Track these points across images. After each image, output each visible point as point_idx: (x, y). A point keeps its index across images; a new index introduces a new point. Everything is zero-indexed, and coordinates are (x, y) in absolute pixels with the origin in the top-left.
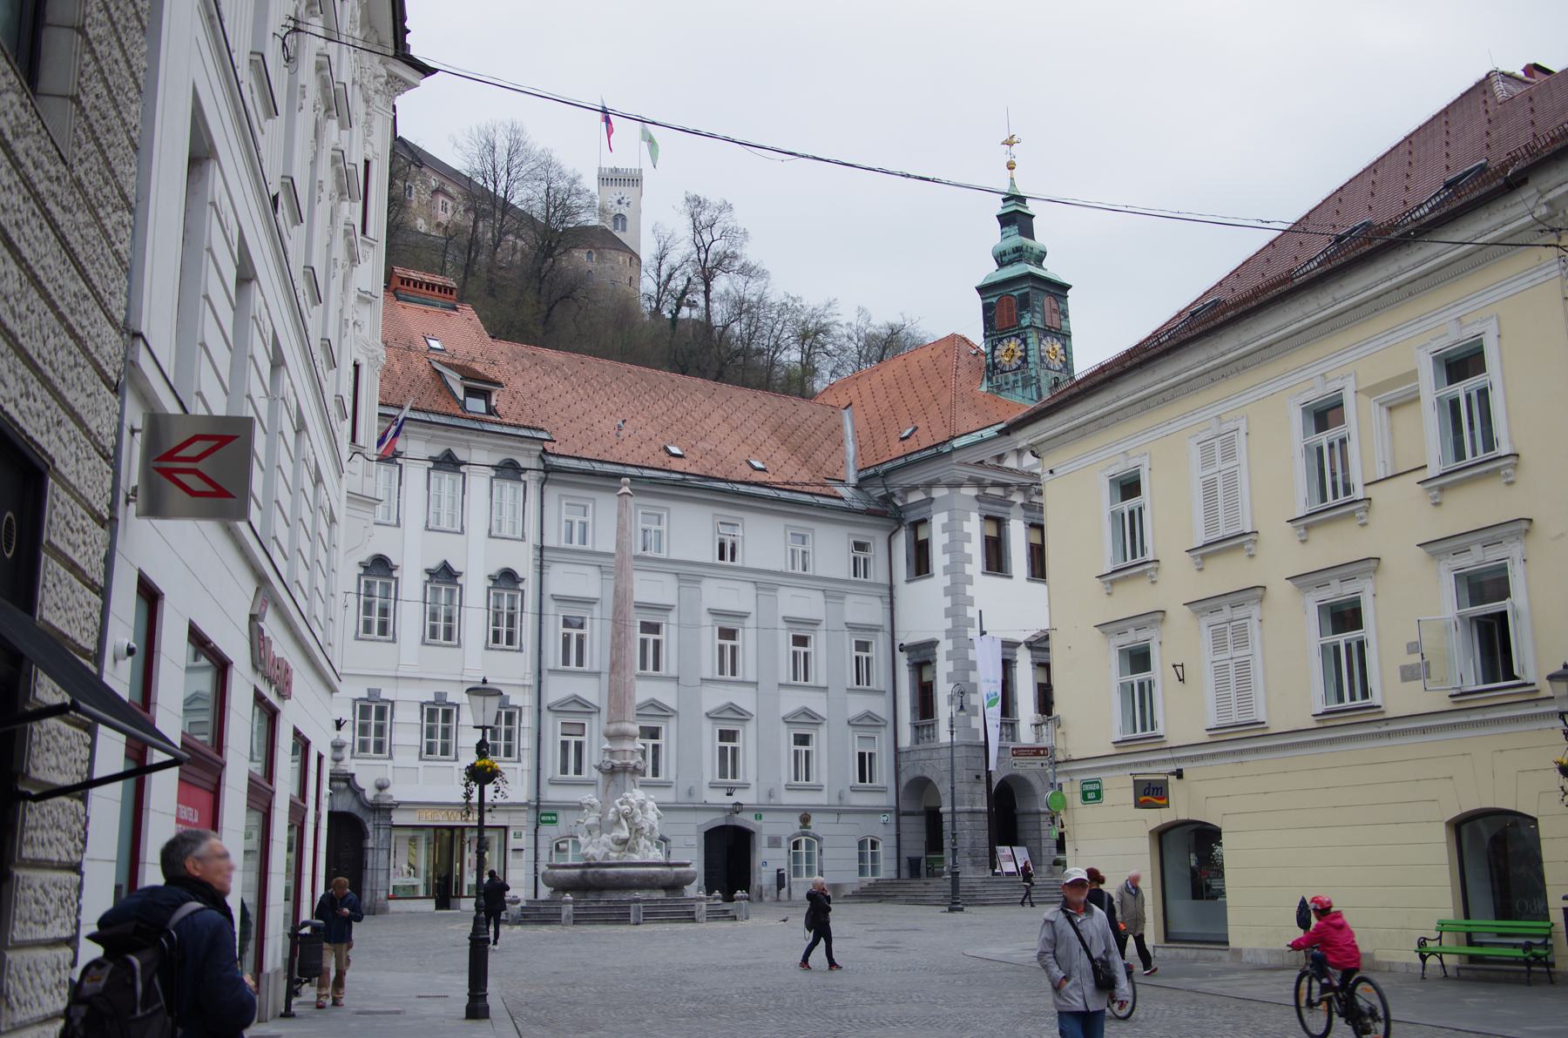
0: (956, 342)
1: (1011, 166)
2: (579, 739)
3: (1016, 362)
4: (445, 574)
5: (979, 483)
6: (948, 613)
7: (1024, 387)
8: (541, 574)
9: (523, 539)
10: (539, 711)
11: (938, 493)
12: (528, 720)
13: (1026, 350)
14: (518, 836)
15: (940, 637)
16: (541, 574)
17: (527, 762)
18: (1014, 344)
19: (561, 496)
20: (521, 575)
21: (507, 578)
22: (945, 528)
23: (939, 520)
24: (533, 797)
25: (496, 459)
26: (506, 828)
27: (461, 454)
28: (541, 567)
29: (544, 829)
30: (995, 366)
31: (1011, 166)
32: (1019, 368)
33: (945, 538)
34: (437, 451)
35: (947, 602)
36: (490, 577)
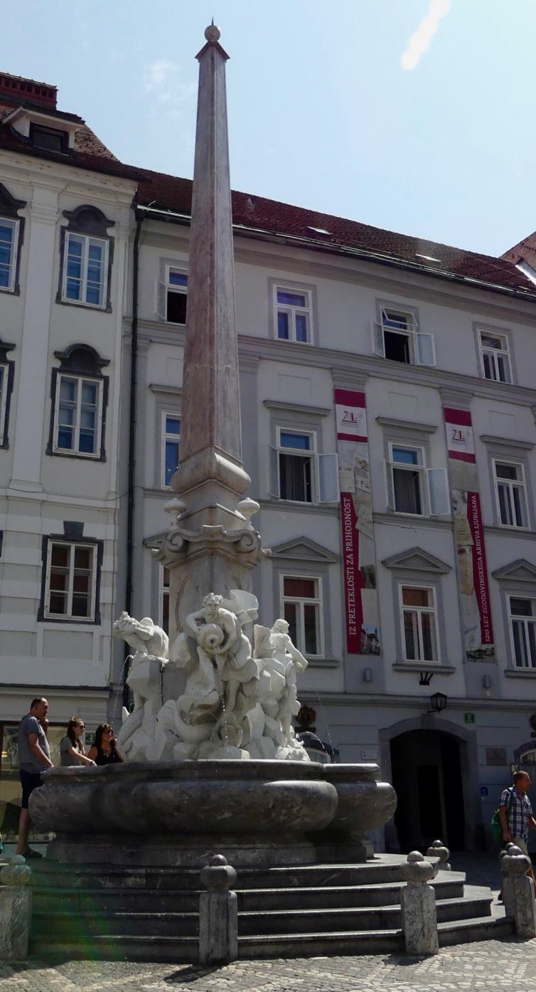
9: (109, 309)
10: (130, 548)
12: (111, 562)
19: (163, 261)
20: (104, 353)
21: (80, 360)
25: (71, 204)
27: (17, 192)
36: (57, 355)
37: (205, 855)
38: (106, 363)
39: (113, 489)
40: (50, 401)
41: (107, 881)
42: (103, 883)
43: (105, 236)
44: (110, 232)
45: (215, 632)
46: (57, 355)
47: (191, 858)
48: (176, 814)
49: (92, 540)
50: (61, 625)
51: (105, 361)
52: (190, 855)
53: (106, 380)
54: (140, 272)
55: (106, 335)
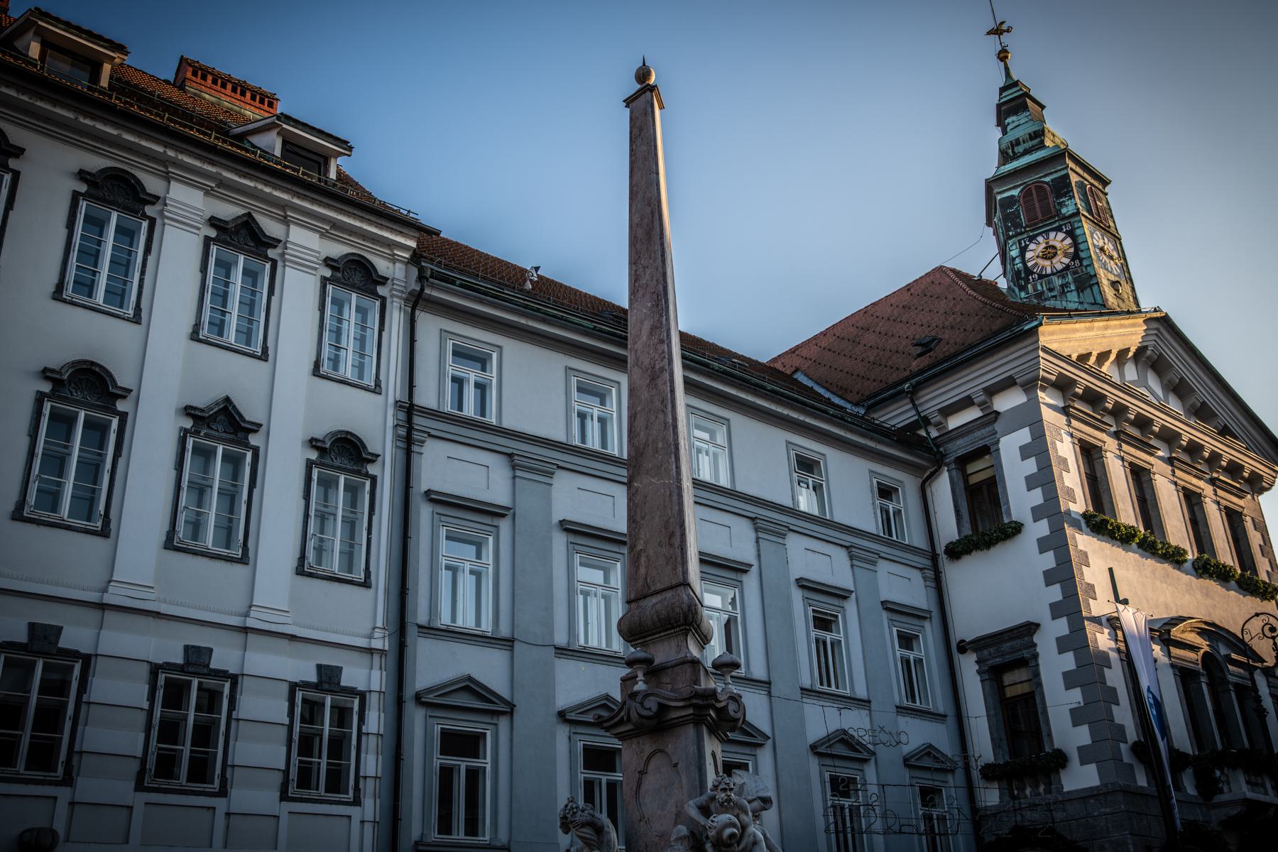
1: (1003, 55)
2: (474, 763)
3: (1060, 261)
4: (222, 428)
5: (1063, 385)
6: (1049, 578)
7: (1080, 289)
8: (408, 453)
10: (400, 702)
11: (1007, 402)
12: (375, 721)
15: (1041, 614)
16: (408, 453)
18: (1059, 240)
20: (373, 447)
23: (1011, 444)
25: (337, 250)
27: (271, 227)
30: (1029, 271)
31: (1003, 55)
32: (1067, 267)
33: (1031, 466)
34: (229, 211)
35: (1049, 560)
38: (373, 458)
39: (379, 624)
40: (302, 502)
43: (375, 295)
44: (381, 290)
45: (733, 825)
46: (313, 443)
50: (310, 805)
51: (372, 454)
53: (374, 479)
54: (417, 345)
55: (373, 420)
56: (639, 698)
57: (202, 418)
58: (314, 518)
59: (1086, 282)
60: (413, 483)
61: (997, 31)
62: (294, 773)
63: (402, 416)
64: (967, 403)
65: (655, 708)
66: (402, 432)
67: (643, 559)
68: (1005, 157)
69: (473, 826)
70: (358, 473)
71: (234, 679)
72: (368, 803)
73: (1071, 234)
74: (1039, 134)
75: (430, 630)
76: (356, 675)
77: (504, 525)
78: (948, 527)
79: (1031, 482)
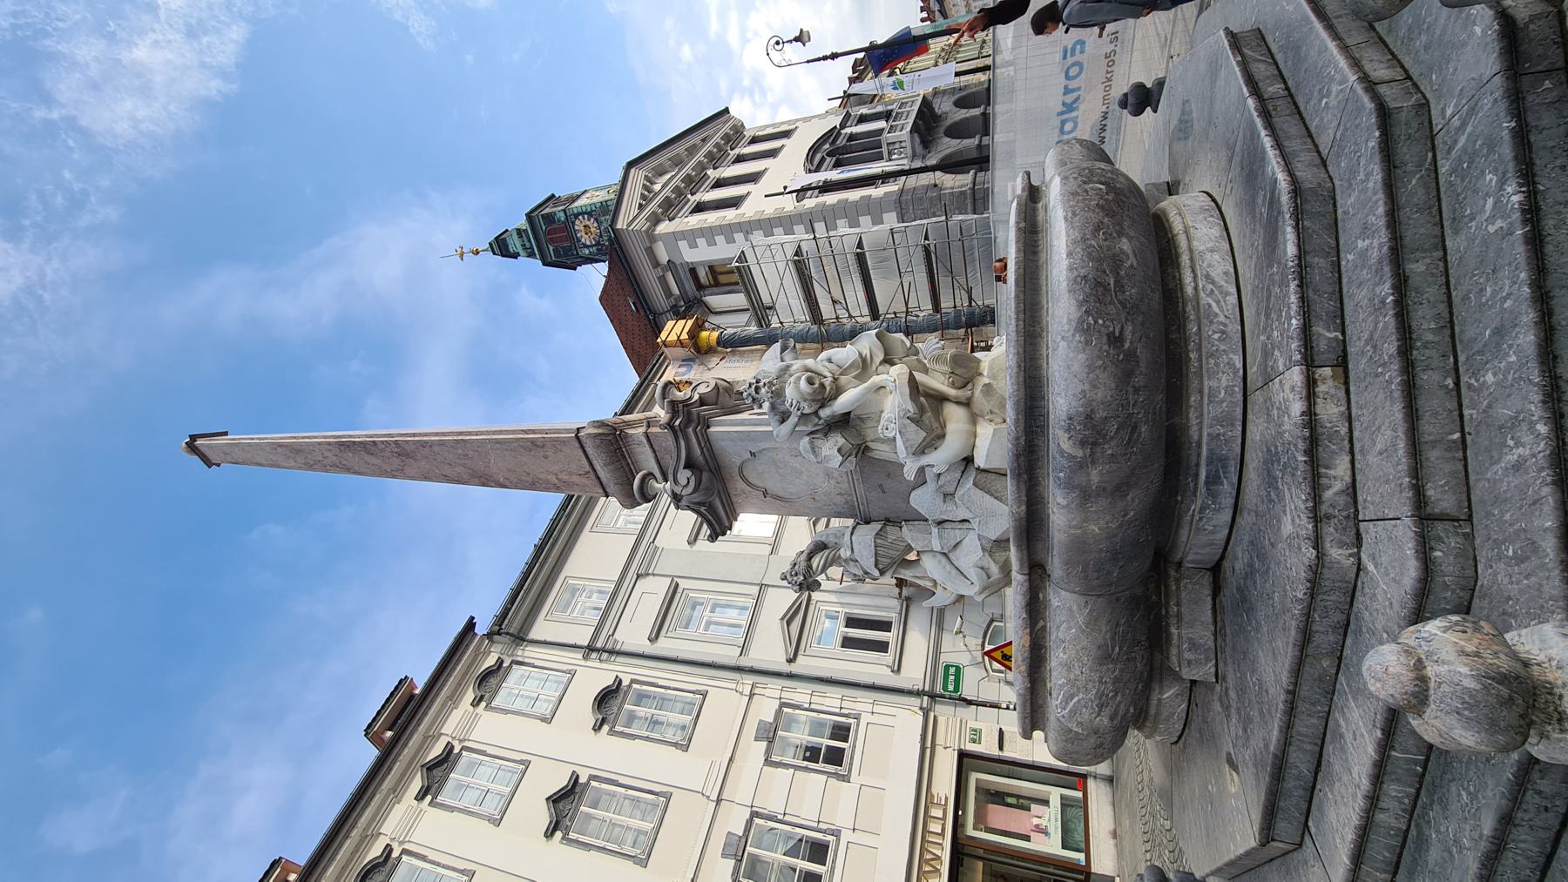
0: (606, 299)
1: (477, 253)
3: (593, 224)
5: (656, 220)
10: (791, 676)
11: (664, 258)
13: (582, 214)
14: (976, 736)
17: (861, 703)
18: (579, 225)
20: (608, 681)
22: (693, 245)
24: (916, 701)
26: (963, 755)
27: (437, 750)
28: (612, 652)
29: (968, 691)
30: (598, 243)
31: (477, 253)
33: (701, 242)
36: (597, 728)
37: (1214, 305)
41: (1332, 472)
42: (1338, 486)
46: (597, 728)
47: (1223, 332)
48: (1127, 345)
49: (779, 713)
52: (1216, 336)
56: (678, 490)
57: (557, 823)
58: (653, 731)
59: (603, 208)
60: (640, 651)
61: (462, 256)
62: (831, 768)
63: (594, 655)
64: (663, 280)
65: (688, 473)
66: (605, 656)
67: (564, 477)
68: (531, 255)
69: (885, 626)
70: (626, 693)
71: (754, 814)
72: (859, 707)
73: (576, 216)
74: (519, 232)
75: (744, 649)
76: (765, 710)
77: (683, 584)
78: (739, 300)
79: (711, 243)
